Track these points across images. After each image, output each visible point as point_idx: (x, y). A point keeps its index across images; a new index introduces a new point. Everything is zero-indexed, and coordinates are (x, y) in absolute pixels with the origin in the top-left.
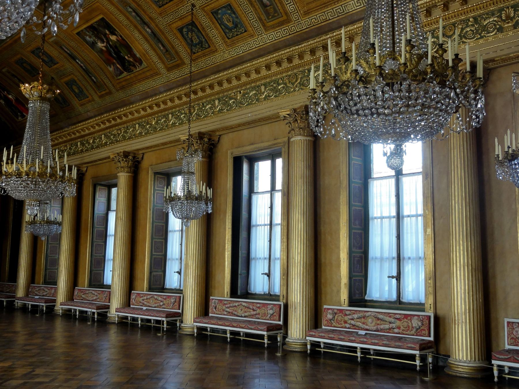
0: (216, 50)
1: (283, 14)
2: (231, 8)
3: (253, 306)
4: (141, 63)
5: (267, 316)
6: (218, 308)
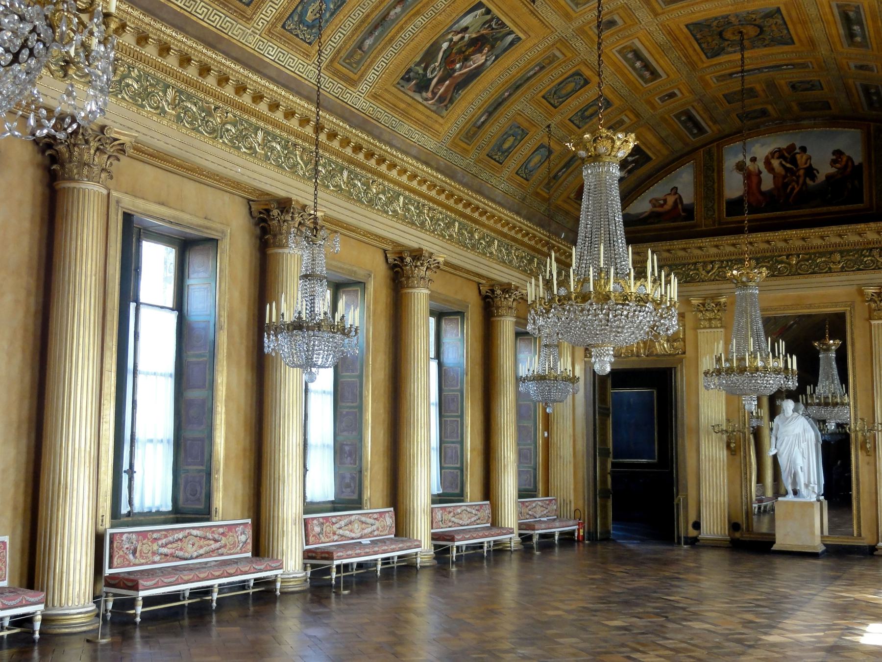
0: (249, 19)
2: (339, 6)
3: (213, 532)
5: (238, 546)
6: (141, 551)
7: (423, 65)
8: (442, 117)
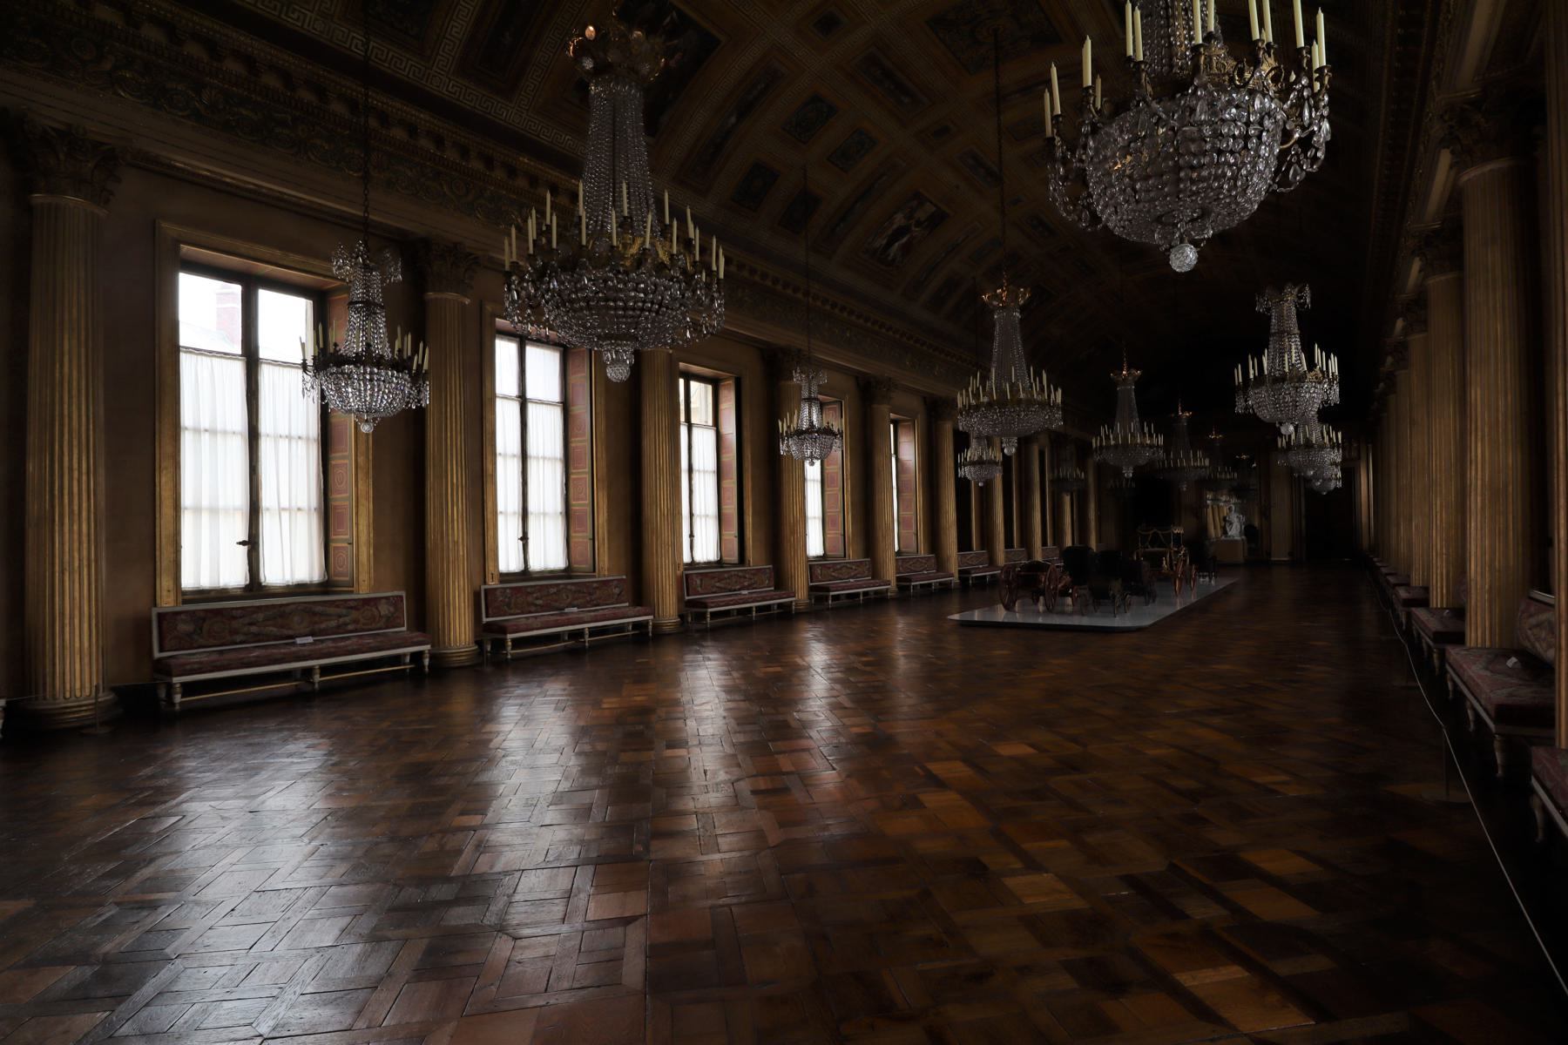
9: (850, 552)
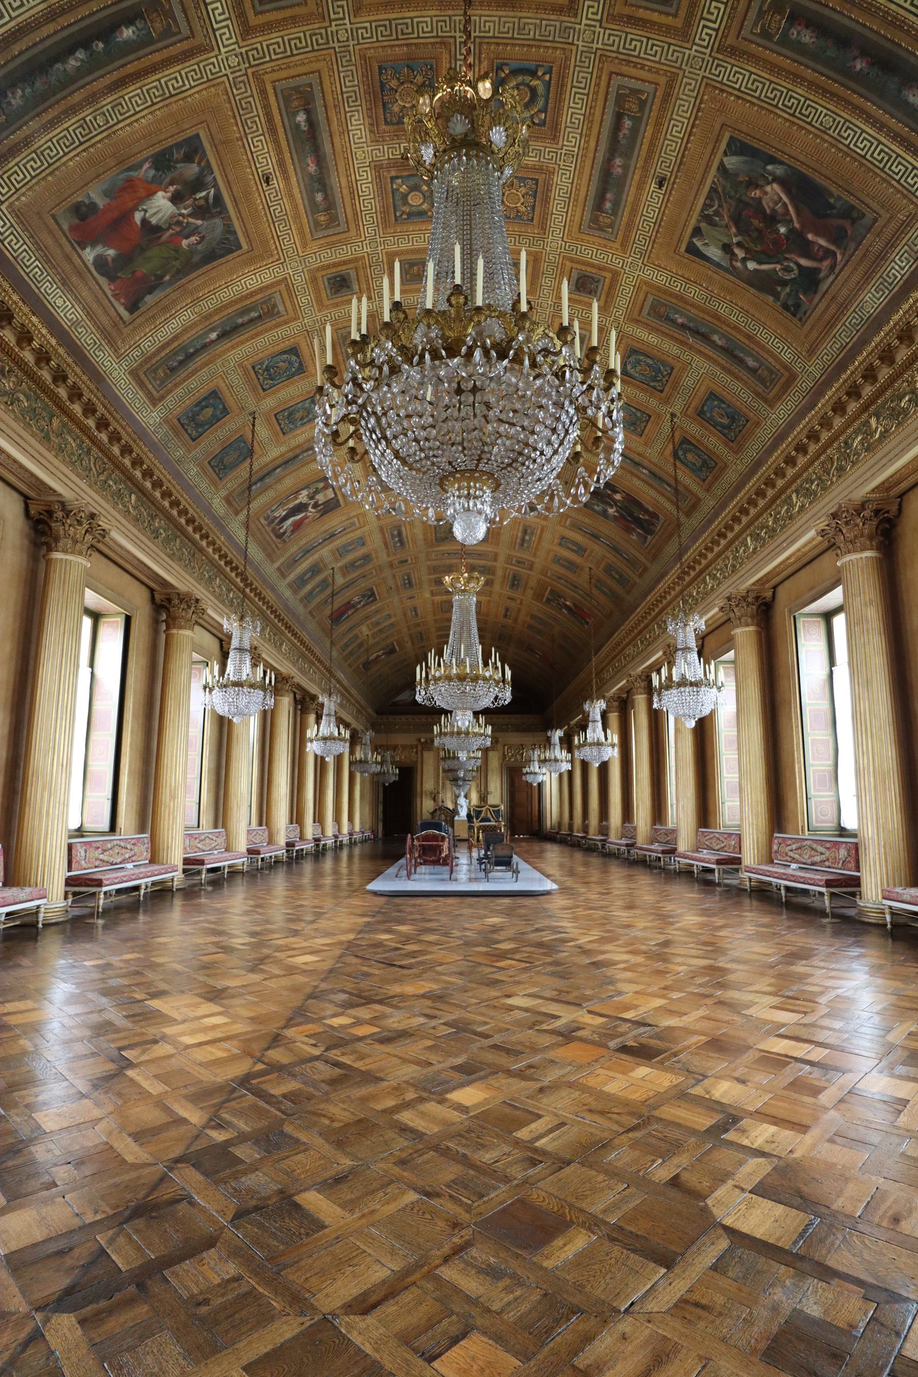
1: (782, 371)
4: (658, 518)
7: (779, 289)
8: (875, 220)
9: (203, 821)
